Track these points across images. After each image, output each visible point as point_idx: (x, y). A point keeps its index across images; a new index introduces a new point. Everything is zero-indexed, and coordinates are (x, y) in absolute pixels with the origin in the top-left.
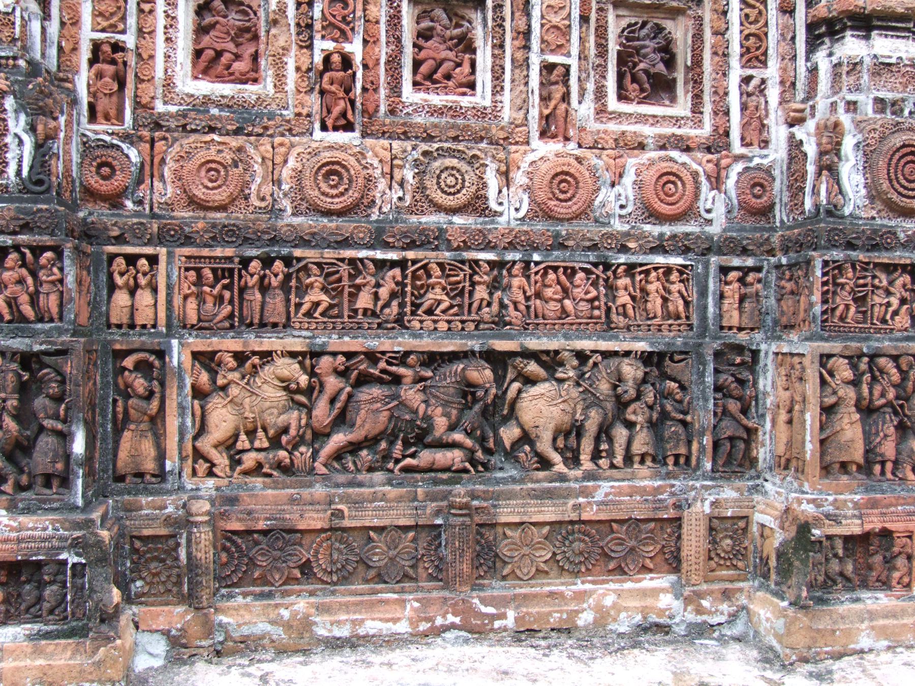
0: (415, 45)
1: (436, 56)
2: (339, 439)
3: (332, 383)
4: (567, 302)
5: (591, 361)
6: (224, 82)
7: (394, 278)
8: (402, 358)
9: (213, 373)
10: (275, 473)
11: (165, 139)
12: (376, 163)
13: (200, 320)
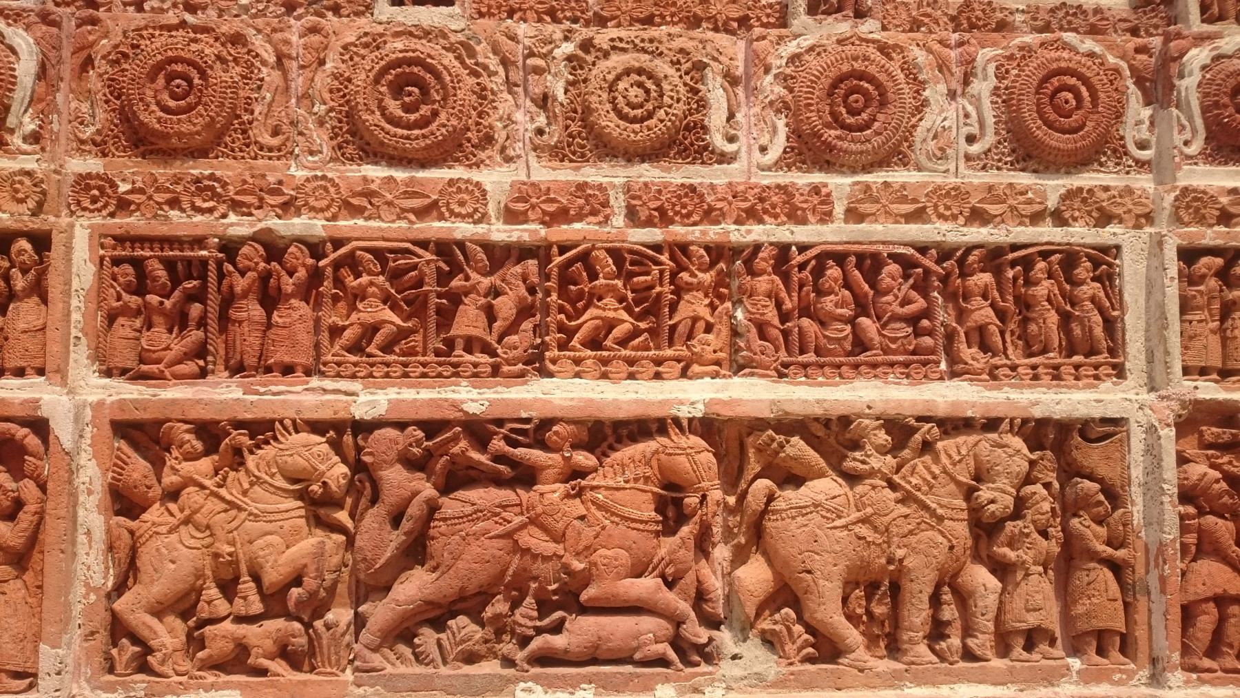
3: (395, 478)
4: (863, 320)
5: (918, 437)
12: (493, 62)
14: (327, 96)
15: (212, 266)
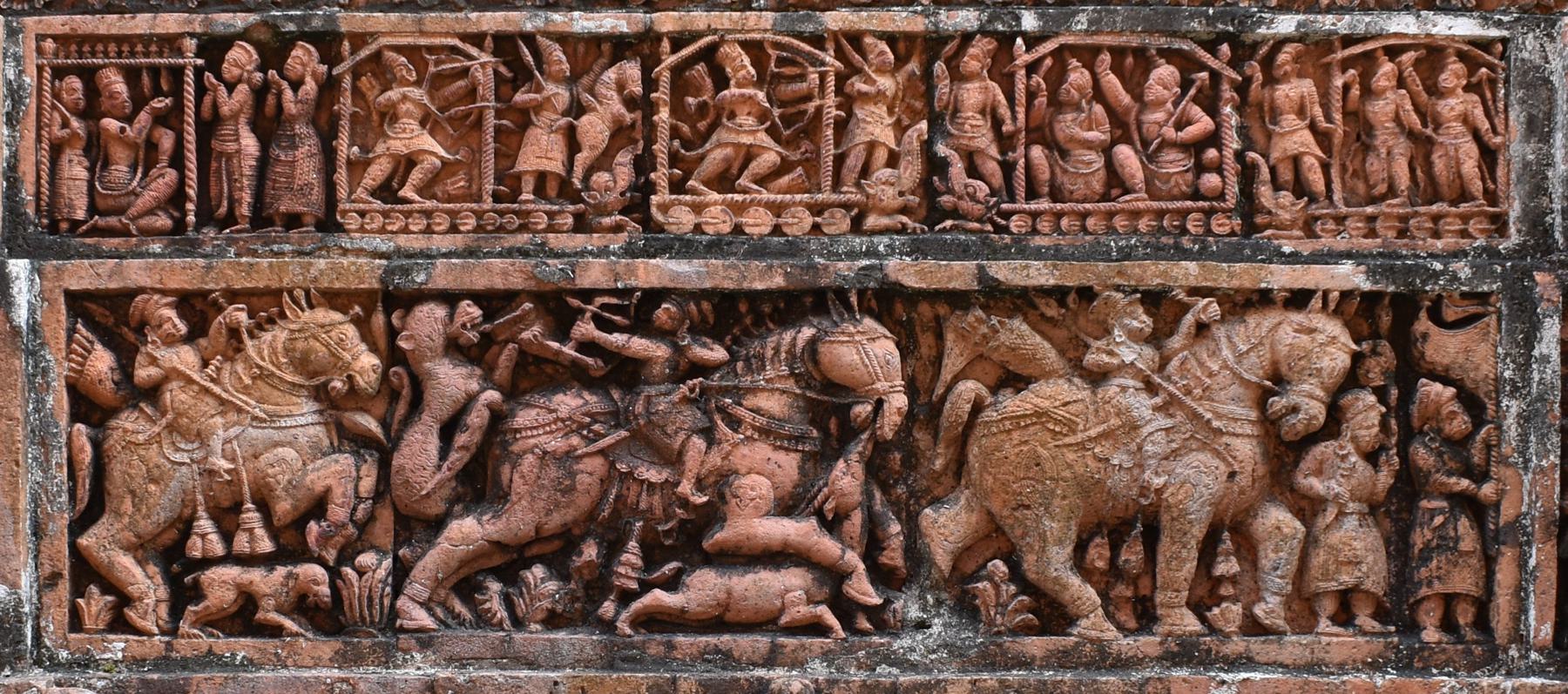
2: (467, 530)
4: (1124, 152)
5: (1189, 319)
7: (621, 86)
8: (639, 310)
9: (126, 357)
10: (289, 624)
13: (93, 209)
15: (190, 77)
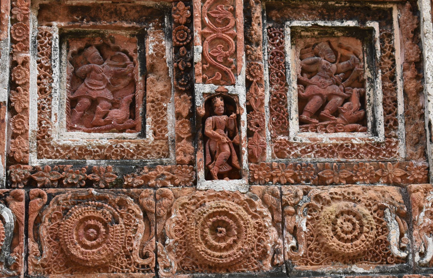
0: (299, 82)
1: (322, 91)
6: (100, 131)
11: (40, 196)
12: (265, 211)
14: (173, 234)
